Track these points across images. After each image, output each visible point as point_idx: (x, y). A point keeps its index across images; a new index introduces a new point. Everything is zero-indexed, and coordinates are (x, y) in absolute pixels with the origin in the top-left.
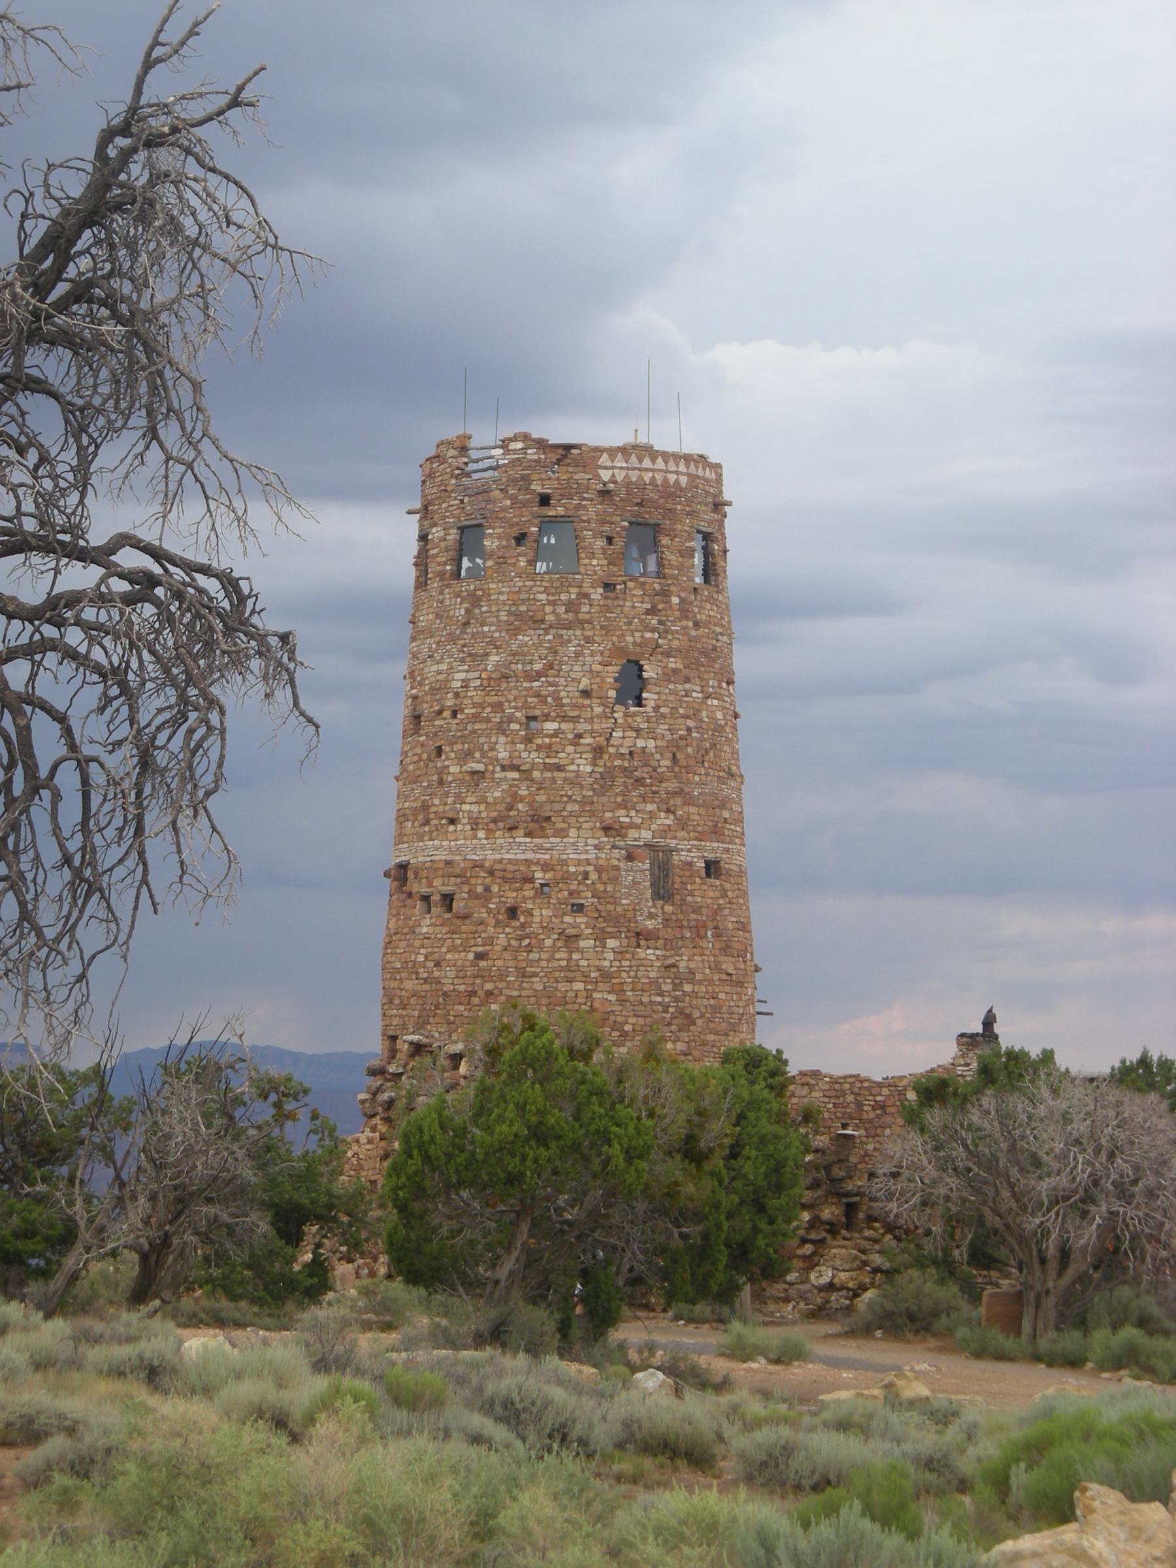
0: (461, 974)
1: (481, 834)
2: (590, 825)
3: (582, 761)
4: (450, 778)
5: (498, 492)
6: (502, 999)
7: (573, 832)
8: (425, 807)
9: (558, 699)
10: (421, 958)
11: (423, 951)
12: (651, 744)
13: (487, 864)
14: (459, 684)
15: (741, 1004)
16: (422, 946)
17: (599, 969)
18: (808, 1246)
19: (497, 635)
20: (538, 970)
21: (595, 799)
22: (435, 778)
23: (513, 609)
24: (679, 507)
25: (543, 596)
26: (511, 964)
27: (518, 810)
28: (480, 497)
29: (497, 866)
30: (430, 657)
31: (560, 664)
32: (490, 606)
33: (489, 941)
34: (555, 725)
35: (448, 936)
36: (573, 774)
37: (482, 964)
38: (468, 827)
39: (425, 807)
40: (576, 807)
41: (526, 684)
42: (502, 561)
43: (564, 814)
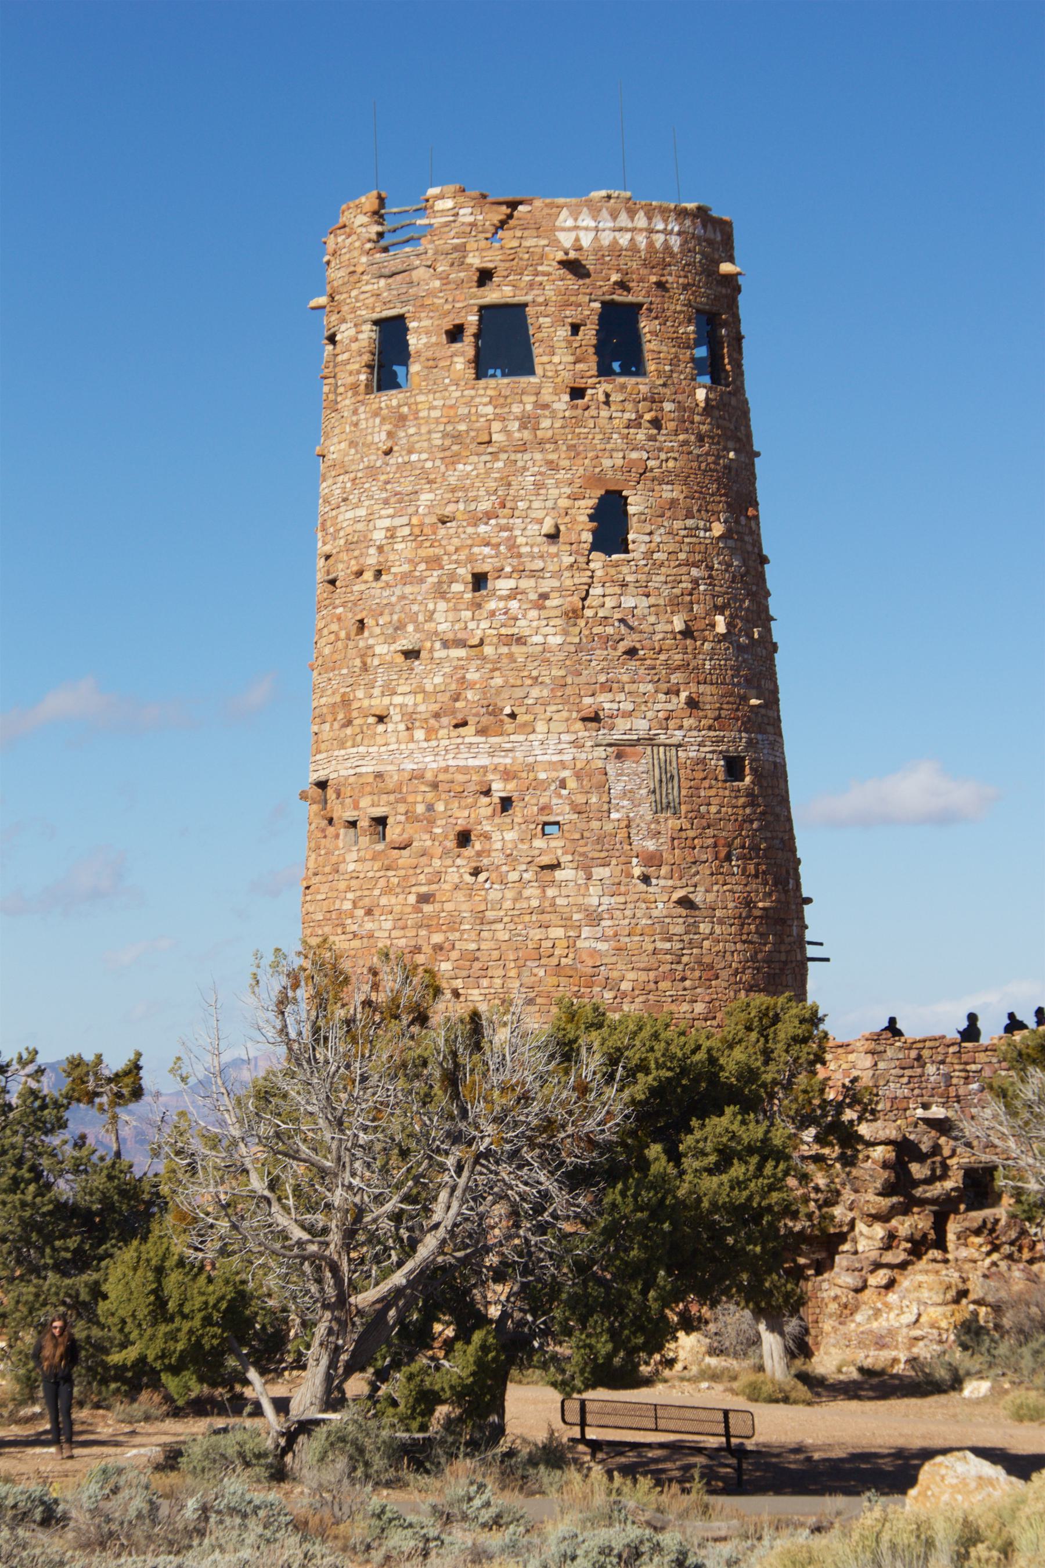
1: (419, 734)
2: (565, 714)
3: (551, 630)
4: (376, 662)
5: (422, 270)
6: (455, 955)
7: (541, 727)
8: (346, 702)
9: (512, 546)
10: (347, 906)
11: (350, 896)
12: (644, 602)
13: (429, 776)
15: (783, 948)
16: (349, 889)
17: (581, 908)
18: (882, 1272)
19: (429, 464)
20: (502, 913)
21: (569, 680)
22: (358, 662)
23: (449, 428)
24: (670, 279)
25: (490, 409)
26: (465, 907)
28: (399, 277)
29: (441, 777)
30: (345, 500)
31: (515, 500)
32: (419, 426)
33: (437, 878)
34: (511, 583)
35: (382, 873)
36: (540, 648)
37: (427, 908)
38: (402, 727)
39: (346, 702)
40: (545, 693)
41: (470, 530)
42: (432, 364)
43: (530, 701)
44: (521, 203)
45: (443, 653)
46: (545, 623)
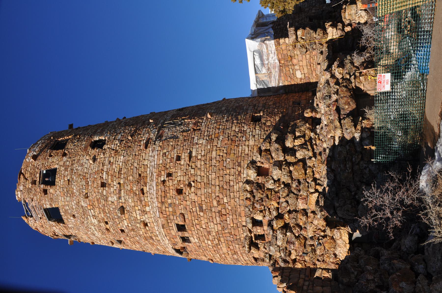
0: (210, 219)
1: (147, 209)
4: (130, 225)
6: (221, 196)
14: (95, 220)
25: (62, 181)
27: (136, 190)
29: (160, 201)
34: (105, 173)
36: (123, 163)
44: (21, 171)
45: (123, 198)
46: (117, 162)
